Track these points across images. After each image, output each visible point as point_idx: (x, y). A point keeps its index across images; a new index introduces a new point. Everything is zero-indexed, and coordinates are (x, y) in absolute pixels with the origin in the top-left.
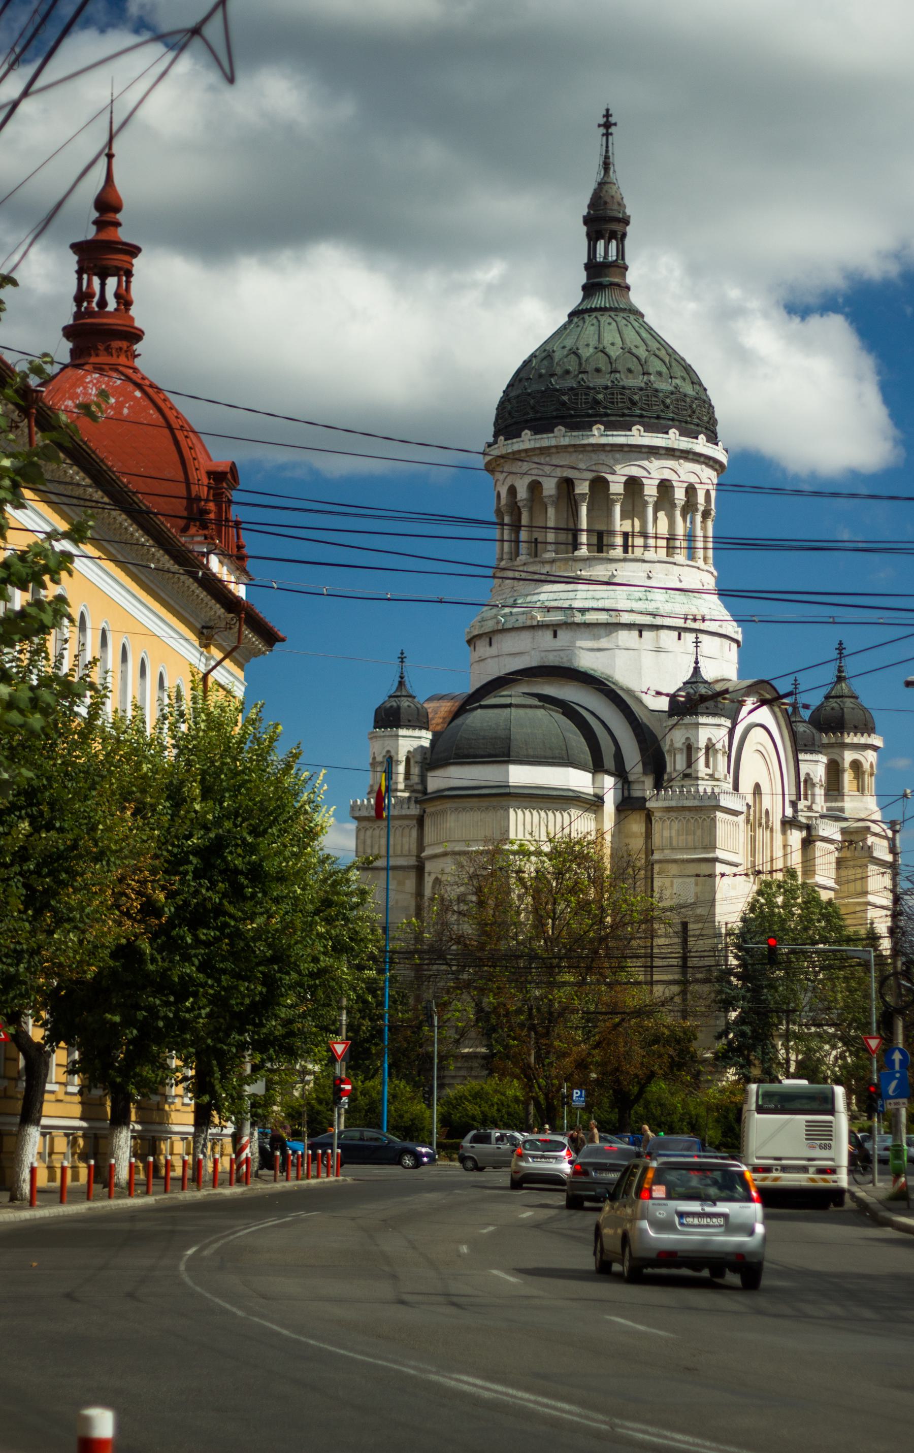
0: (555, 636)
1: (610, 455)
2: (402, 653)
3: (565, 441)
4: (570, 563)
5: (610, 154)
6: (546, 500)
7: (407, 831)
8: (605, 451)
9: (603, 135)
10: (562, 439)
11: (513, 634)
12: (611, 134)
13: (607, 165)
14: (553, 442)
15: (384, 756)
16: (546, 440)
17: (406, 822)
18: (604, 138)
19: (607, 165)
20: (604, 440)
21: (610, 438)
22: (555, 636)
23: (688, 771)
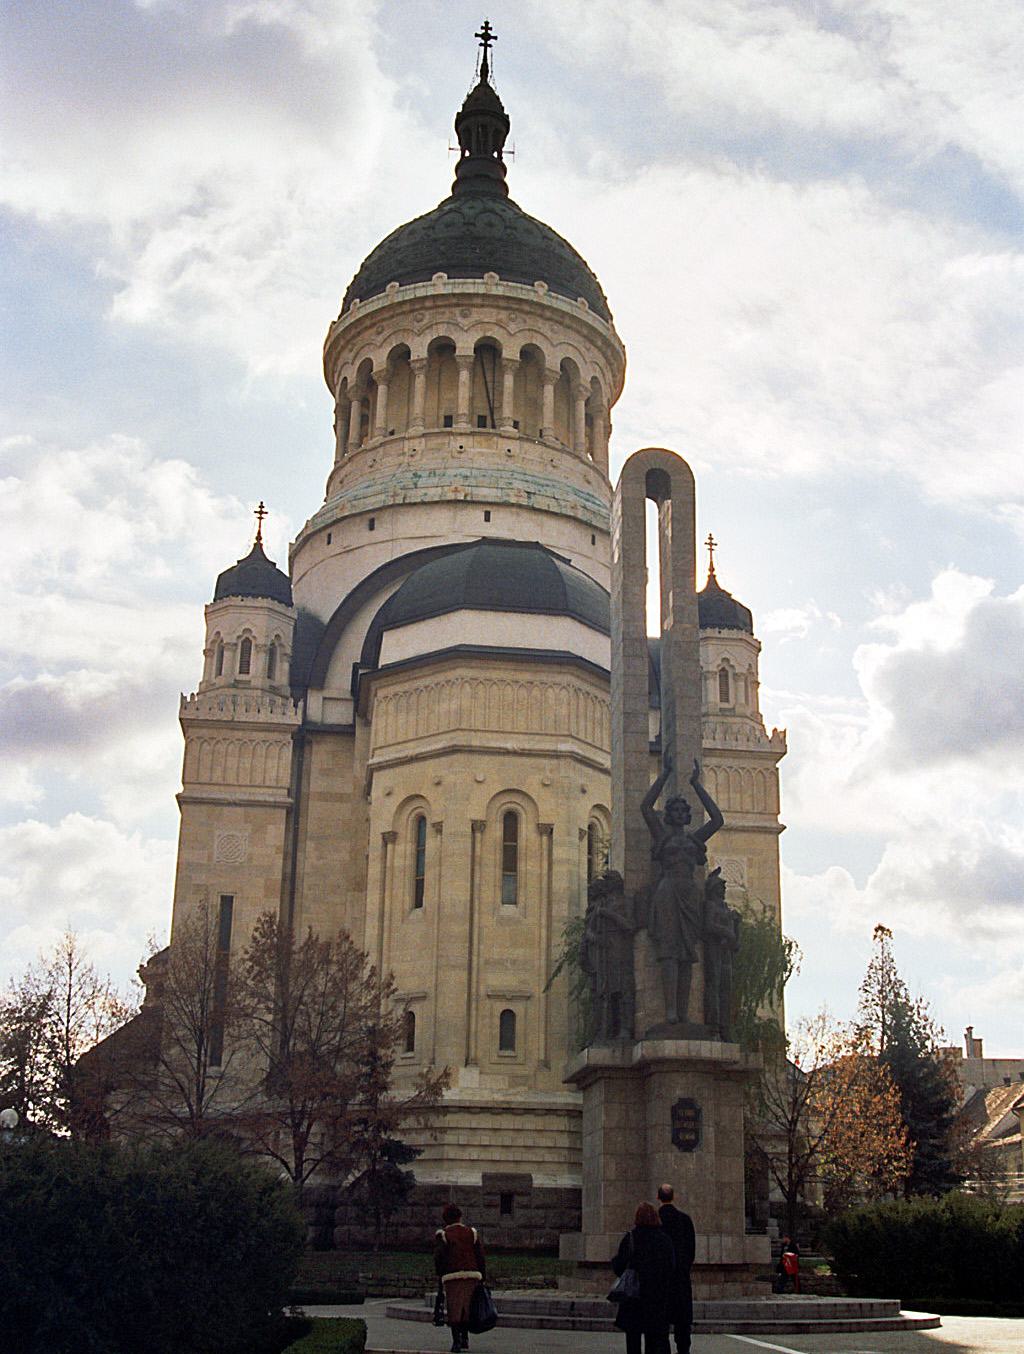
0: (487, 519)
1: (548, 324)
2: (262, 507)
3: (499, 291)
4: (495, 438)
5: (489, 62)
6: (458, 360)
7: (275, 750)
8: (541, 316)
9: (481, 45)
10: (494, 288)
11: (421, 512)
12: (490, 46)
13: (484, 71)
14: (482, 290)
15: (239, 637)
16: (472, 286)
17: (275, 736)
18: (483, 48)
19: (484, 71)
20: (546, 301)
21: (554, 301)
22: (487, 519)
23: (725, 705)
